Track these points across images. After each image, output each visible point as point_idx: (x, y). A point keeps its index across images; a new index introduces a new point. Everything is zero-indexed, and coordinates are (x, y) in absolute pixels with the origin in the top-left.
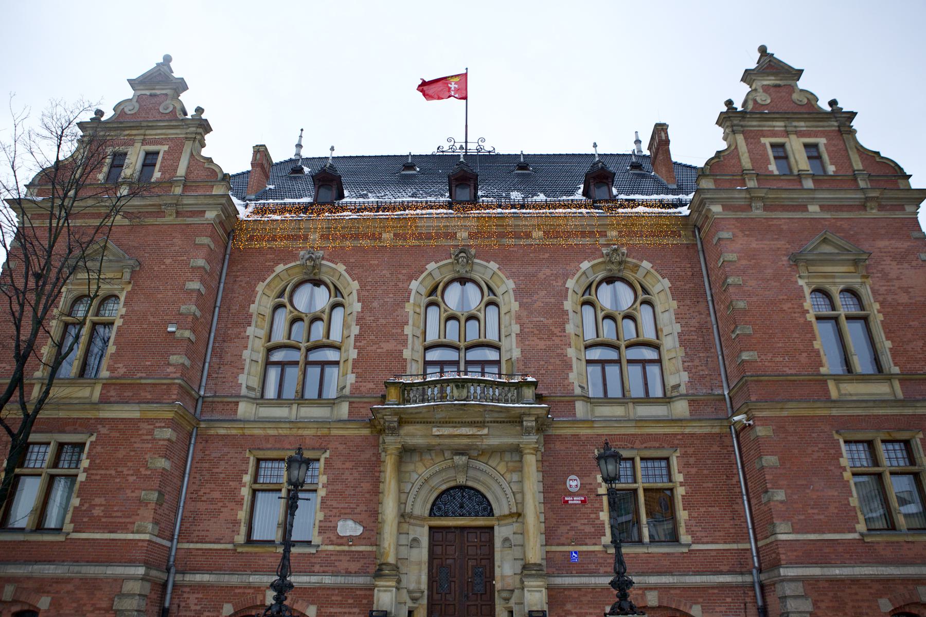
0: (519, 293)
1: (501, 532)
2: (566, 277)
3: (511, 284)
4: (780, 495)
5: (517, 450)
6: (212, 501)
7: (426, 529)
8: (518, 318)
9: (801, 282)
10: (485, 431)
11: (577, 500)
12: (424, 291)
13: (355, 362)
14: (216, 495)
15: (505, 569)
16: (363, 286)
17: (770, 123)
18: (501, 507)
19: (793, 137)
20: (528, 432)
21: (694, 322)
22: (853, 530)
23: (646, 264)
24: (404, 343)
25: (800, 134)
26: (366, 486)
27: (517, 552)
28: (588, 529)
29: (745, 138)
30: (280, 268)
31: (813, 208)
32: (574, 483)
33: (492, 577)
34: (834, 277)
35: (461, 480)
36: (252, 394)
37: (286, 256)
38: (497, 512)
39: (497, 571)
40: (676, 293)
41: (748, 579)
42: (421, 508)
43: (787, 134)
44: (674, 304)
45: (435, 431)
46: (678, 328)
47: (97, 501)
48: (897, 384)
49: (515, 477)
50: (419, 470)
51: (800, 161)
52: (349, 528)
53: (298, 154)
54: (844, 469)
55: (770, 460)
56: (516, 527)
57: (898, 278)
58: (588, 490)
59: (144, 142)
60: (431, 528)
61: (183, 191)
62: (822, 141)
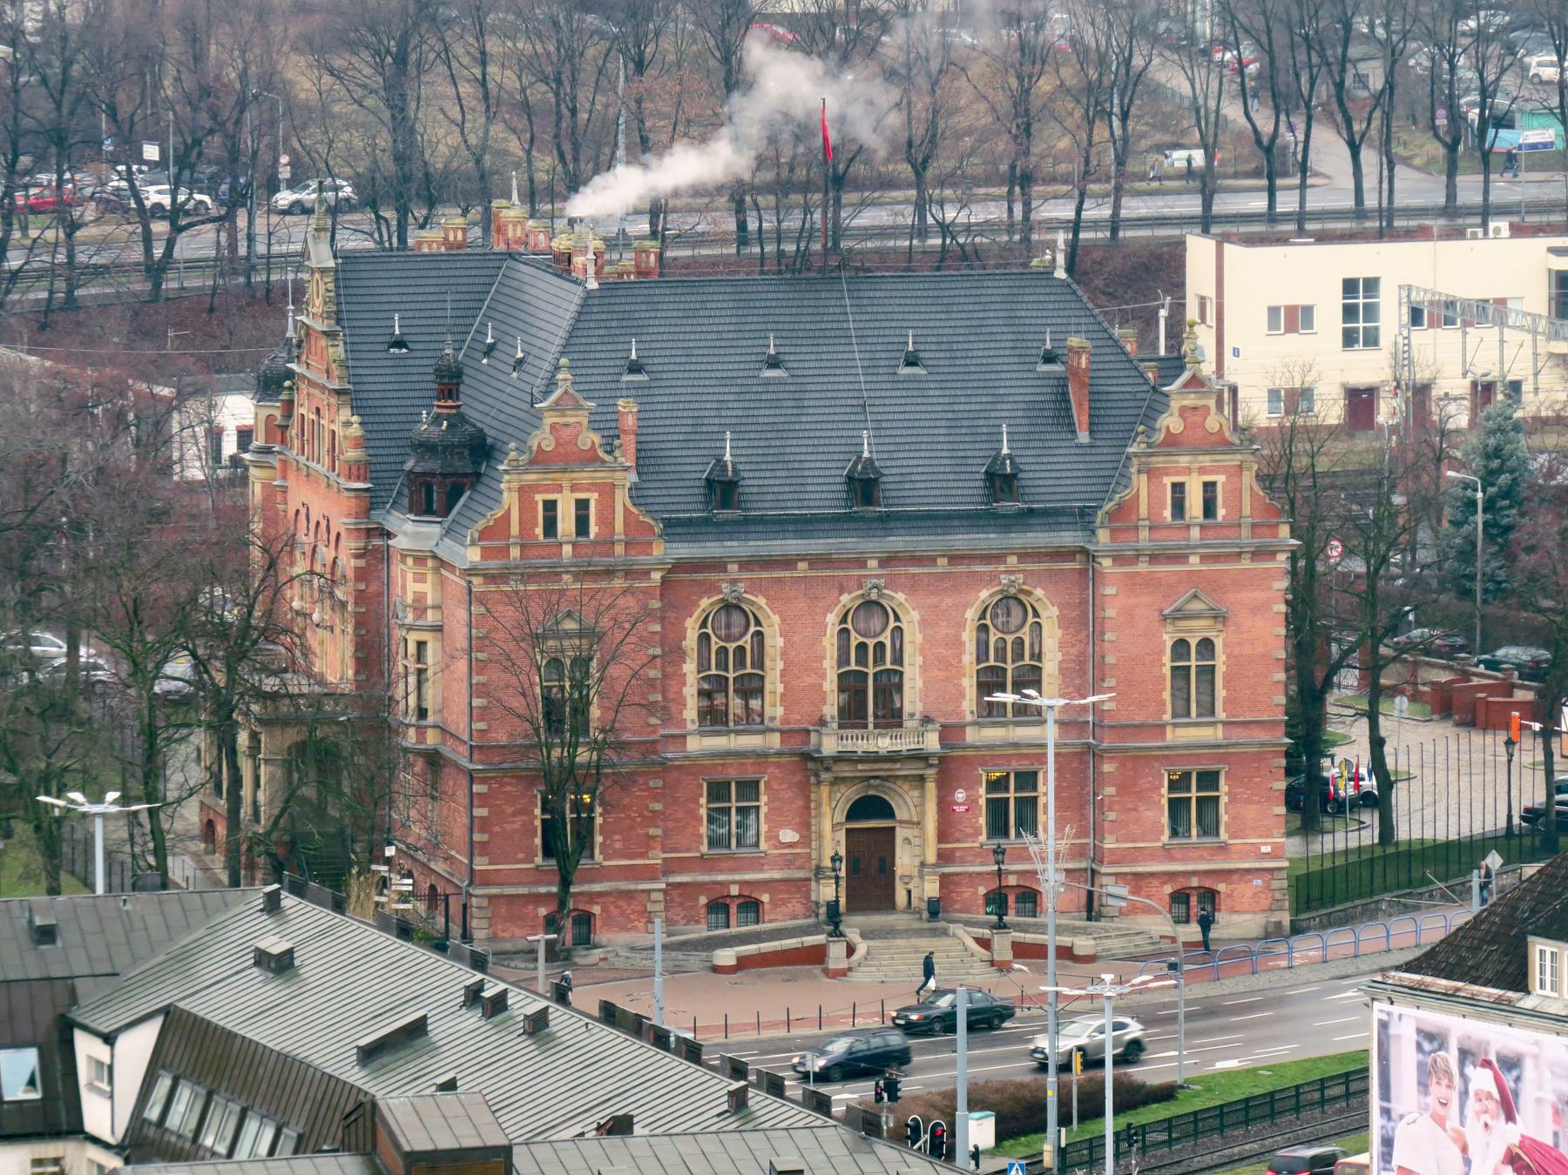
0: (924, 623)
1: (900, 833)
2: (966, 606)
3: (915, 616)
4: (1112, 816)
5: (922, 779)
6: (676, 820)
8: (922, 651)
9: (1166, 637)
11: (963, 808)
12: (837, 620)
13: (783, 695)
14: (680, 815)
15: (904, 861)
16: (783, 620)
18: (900, 814)
19: (1195, 475)
20: (931, 766)
21: (1074, 651)
23: (1039, 592)
24: (824, 677)
25: (1202, 471)
26: (800, 803)
27: (917, 851)
28: (968, 830)
30: (705, 602)
31: (1194, 559)
33: (893, 864)
35: (871, 792)
37: (712, 588)
38: (898, 815)
39: (898, 861)
40: (1063, 621)
41: (1083, 865)
42: (840, 817)
43: (1188, 471)
44: (1059, 633)
45: (860, 767)
46: (1059, 656)
47: (617, 837)
49: (916, 793)
52: (789, 835)
55: (1110, 790)
56: (916, 832)
58: (971, 803)
59: (574, 488)
60: (848, 831)
62: (1220, 479)
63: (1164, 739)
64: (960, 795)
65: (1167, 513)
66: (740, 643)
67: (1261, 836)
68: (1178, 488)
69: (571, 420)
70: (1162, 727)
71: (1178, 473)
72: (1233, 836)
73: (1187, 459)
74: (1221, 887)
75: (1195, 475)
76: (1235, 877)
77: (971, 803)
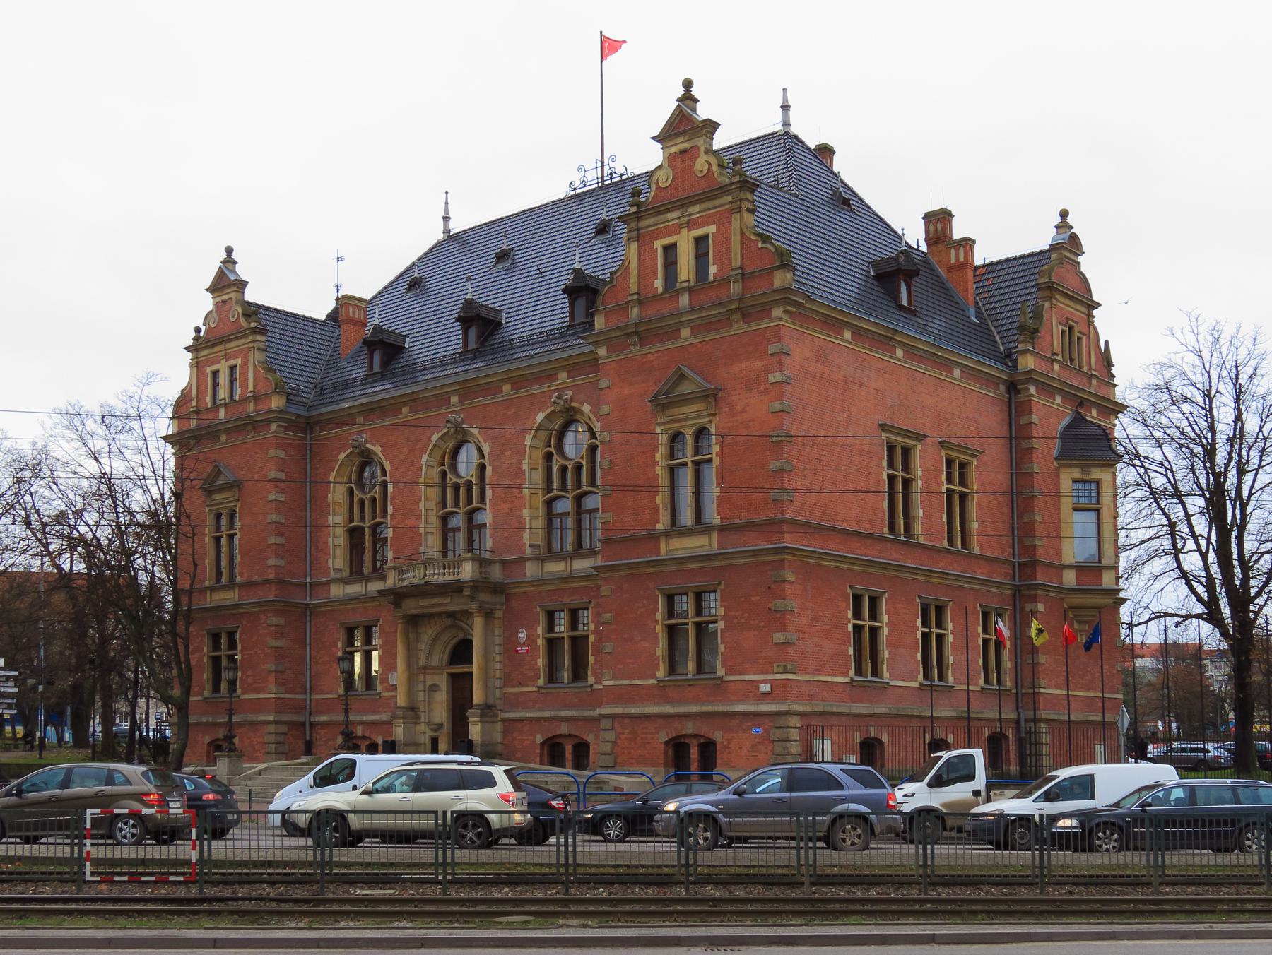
7: (445, 676)
10: (449, 600)
11: (524, 649)
17: (666, 216)
22: (654, 676)
25: (690, 225)
28: (531, 674)
29: (639, 246)
31: (685, 333)
32: (521, 635)
34: (686, 420)
36: (339, 575)
43: (676, 230)
48: (715, 535)
50: (428, 632)
51: (686, 268)
53: (447, 231)
54: (657, 622)
57: (744, 411)
58: (531, 640)
61: (256, 405)
62: (711, 229)
63: (658, 554)
64: (522, 635)
65: (659, 284)
66: (372, 494)
67: (763, 673)
68: (670, 249)
69: (225, 297)
70: (655, 537)
71: (669, 234)
72: (728, 673)
73: (674, 215)
74: (718, 736)
75: (684, 232)
76: (734, 723)
77: (531, 640)
